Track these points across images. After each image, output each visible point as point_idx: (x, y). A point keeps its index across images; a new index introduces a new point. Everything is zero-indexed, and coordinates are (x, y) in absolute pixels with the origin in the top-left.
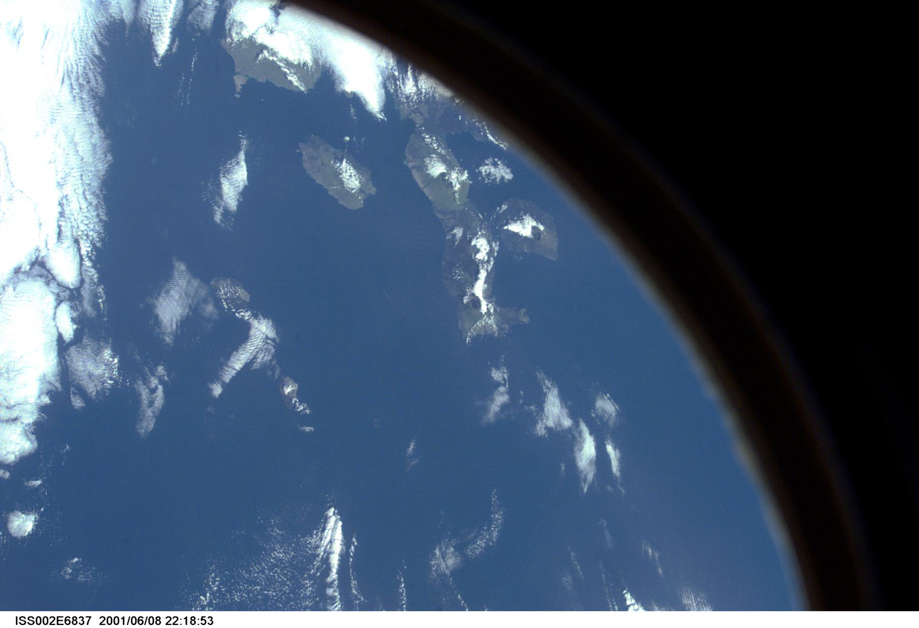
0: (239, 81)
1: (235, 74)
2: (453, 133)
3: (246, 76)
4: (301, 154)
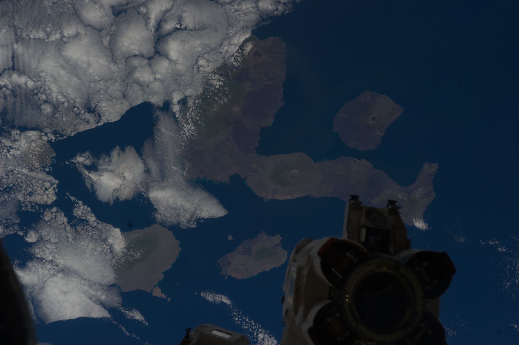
0: (157, 293)
1: (151, 294)
3: (155, 286)
4: (230, 277)
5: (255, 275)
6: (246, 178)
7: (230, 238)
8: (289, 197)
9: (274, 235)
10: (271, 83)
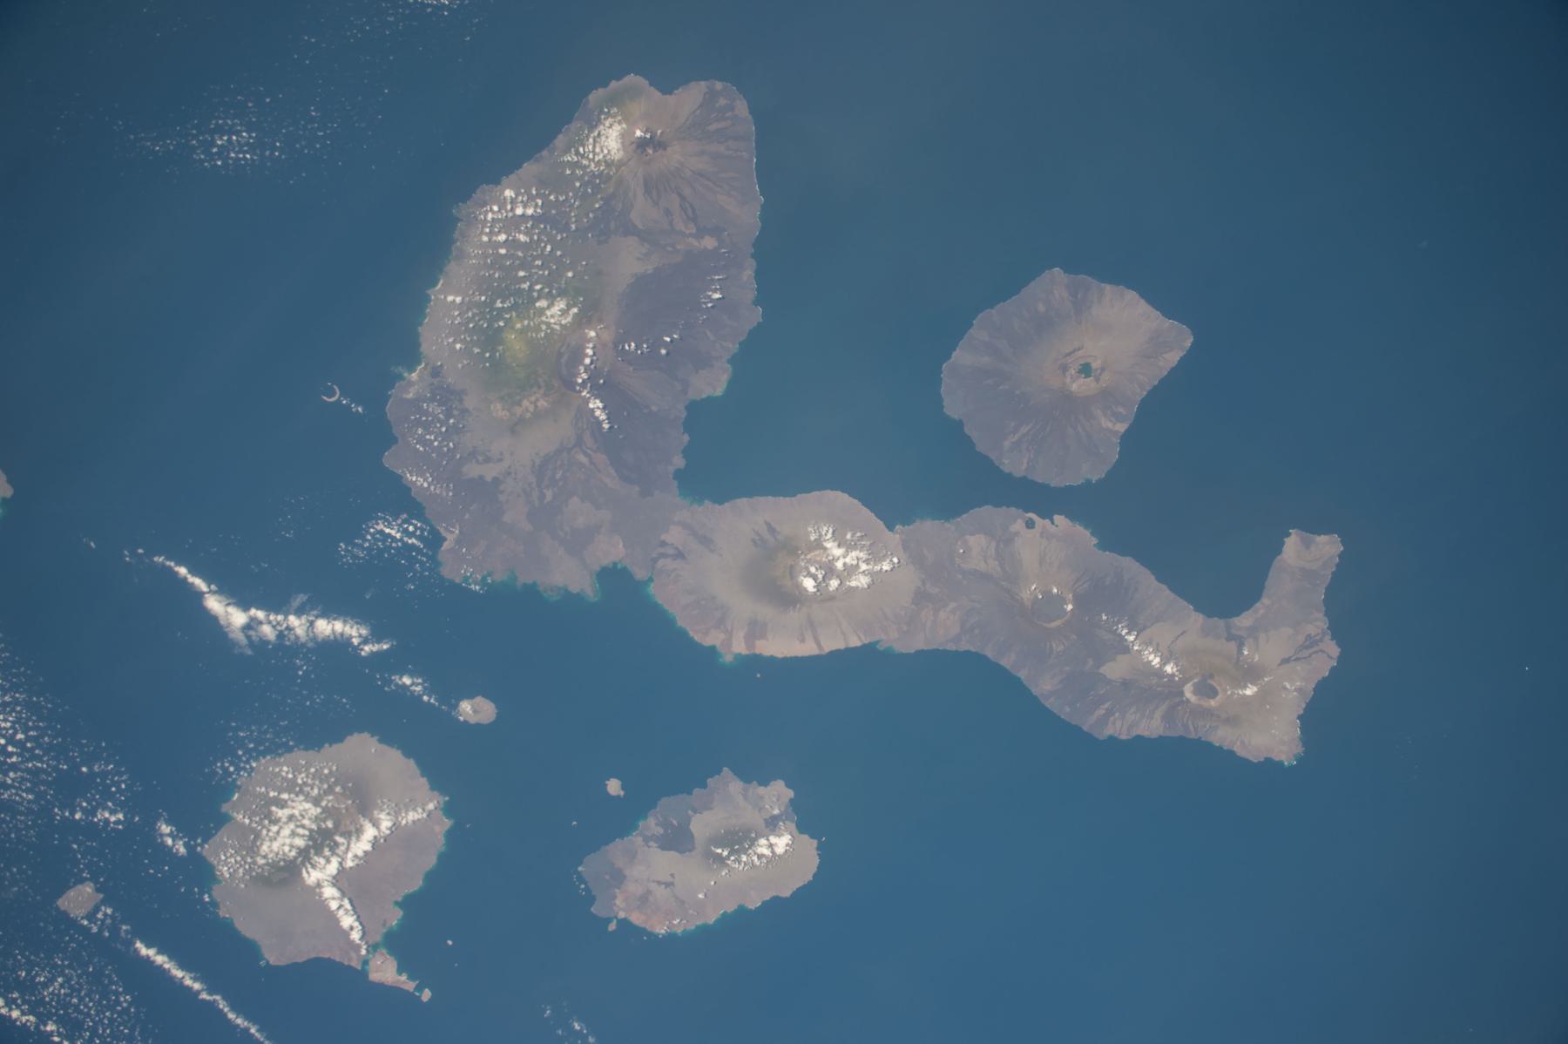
2: (679, 462)
4: (625, 924)
5: (711, 921)
6: (651, 579)
7: (614, 787)
8: (807, 649)
9: (764, 783)
10: (709, 243)
